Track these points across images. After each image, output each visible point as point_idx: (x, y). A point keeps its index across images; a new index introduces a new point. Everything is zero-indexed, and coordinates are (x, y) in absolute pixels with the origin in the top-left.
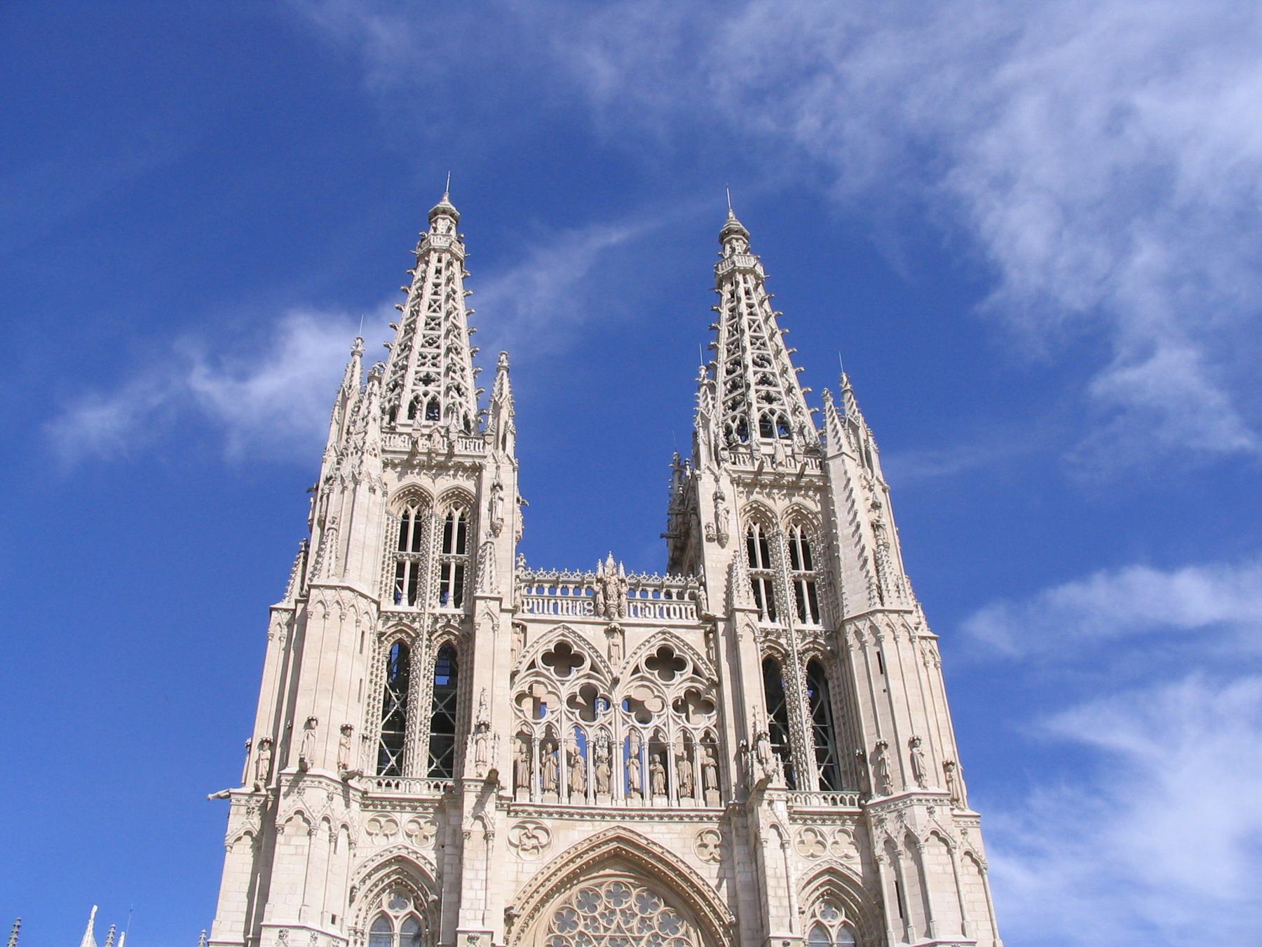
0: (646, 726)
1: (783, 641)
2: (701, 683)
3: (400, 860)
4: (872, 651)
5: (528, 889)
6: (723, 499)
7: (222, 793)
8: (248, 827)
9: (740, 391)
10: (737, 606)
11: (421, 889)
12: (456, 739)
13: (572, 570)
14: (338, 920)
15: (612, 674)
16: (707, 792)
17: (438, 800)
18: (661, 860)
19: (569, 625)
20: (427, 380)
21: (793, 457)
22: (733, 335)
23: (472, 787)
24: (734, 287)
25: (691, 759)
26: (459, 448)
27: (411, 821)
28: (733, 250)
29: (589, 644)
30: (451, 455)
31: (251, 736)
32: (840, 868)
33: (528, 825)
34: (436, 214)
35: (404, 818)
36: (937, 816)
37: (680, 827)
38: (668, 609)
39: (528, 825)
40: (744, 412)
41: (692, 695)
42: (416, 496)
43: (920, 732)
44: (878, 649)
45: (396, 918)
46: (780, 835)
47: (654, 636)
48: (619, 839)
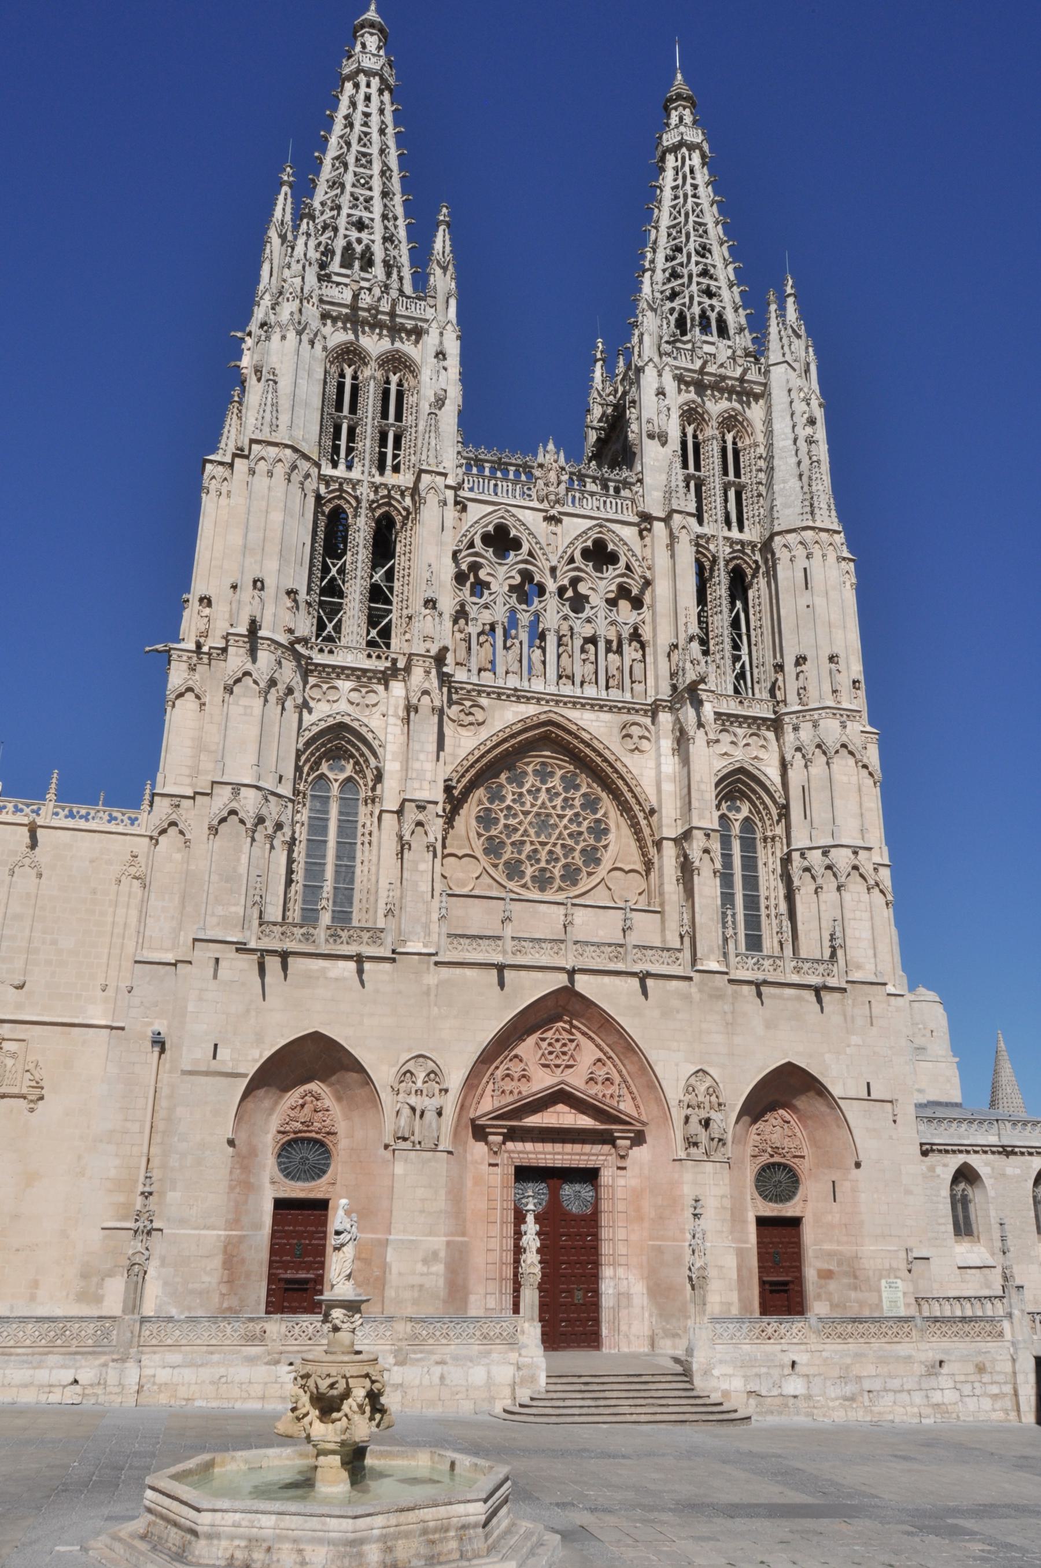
0: (580, 615)
1: (712, 547)
2: (633, 579)
3: (342, 726)
4: (801, 563)
5: (465, 762)
6: (664, 395)
7: (160, 647)
8: (190, 682)
9: (680, 281)
10: (675, 507)
11: (362, 755)
12: (394, 611)
13: (513, 452)
14: (283, 781)
17: (381, 672)
18: (588, 745)
19: (509, 508)
20: (360, 225)
21: (734, 360)
22: (675, 218)
23: (421, 662)
24: (679, 163)
25: (619, 651)
26: (400, 310)
28: (681, 119)
29: (528, 529)
30: (392, 314)
31: (188, 590)
32: (750, 768)
34: (362, 27)
35: (345, 685)
36: (848, 730)
37: (606, 717)
38: (605, 502)
39: (465, 702)
40: (684, 304)
42: (350, 354)
44: (806, 563)
45: (336, 780)
46: (706, 734)
47: (590, 529)
48: (550, 723)
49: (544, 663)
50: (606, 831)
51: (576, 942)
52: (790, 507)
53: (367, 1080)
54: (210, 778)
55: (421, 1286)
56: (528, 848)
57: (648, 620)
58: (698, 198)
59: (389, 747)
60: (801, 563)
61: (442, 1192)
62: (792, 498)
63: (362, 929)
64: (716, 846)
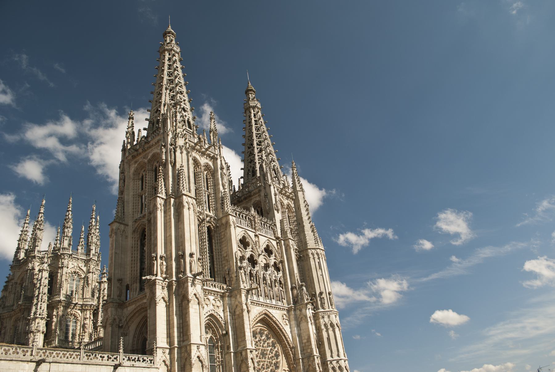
3: (211, 315)
4: (317, 260)
11: (216, 327)
15: (258, 252)
16: (283, 299)
22: (257, 131)
27: (213, 300)
29: (252, 239)
35: (211, 298)
37: (278, 311)
41: (275, 263)
43: (330, 291)
48: (265, 314)
49: (261, 290)
50: (279, 355)
52: (311, 240)
56: (262, 363)
60: (317, 260)
62: (311, 237)
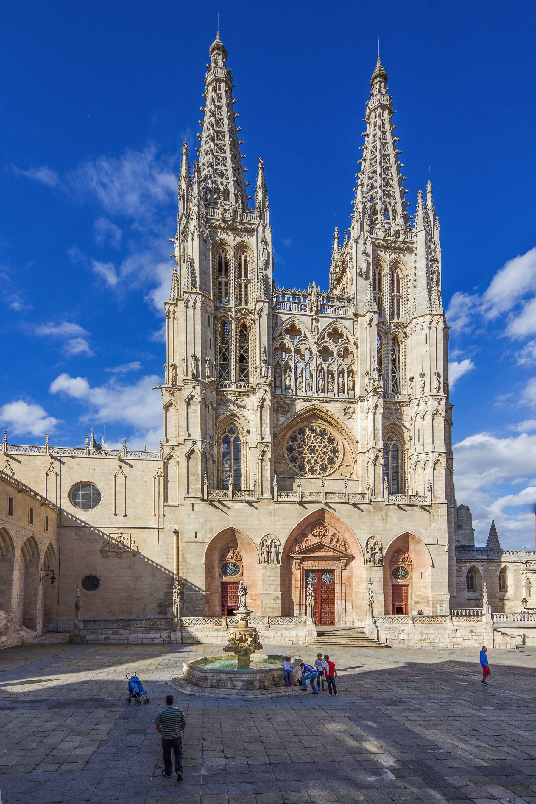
5: (281, 427)
33: (281, 403)
47: (331, 323)
48: (315, 409)
51: (326, 493)
53: (249, 544)
54: (184, 438)
55: (273, 607)
57: (356, 362)
58: (386, 140)
59: (250, 422)
61: (279, 578)
63: (245, 491)
64: (381, 455)
